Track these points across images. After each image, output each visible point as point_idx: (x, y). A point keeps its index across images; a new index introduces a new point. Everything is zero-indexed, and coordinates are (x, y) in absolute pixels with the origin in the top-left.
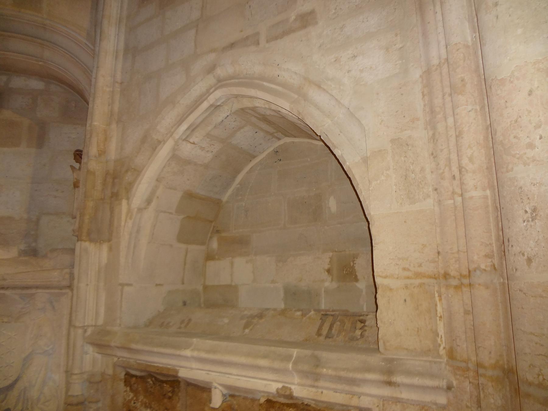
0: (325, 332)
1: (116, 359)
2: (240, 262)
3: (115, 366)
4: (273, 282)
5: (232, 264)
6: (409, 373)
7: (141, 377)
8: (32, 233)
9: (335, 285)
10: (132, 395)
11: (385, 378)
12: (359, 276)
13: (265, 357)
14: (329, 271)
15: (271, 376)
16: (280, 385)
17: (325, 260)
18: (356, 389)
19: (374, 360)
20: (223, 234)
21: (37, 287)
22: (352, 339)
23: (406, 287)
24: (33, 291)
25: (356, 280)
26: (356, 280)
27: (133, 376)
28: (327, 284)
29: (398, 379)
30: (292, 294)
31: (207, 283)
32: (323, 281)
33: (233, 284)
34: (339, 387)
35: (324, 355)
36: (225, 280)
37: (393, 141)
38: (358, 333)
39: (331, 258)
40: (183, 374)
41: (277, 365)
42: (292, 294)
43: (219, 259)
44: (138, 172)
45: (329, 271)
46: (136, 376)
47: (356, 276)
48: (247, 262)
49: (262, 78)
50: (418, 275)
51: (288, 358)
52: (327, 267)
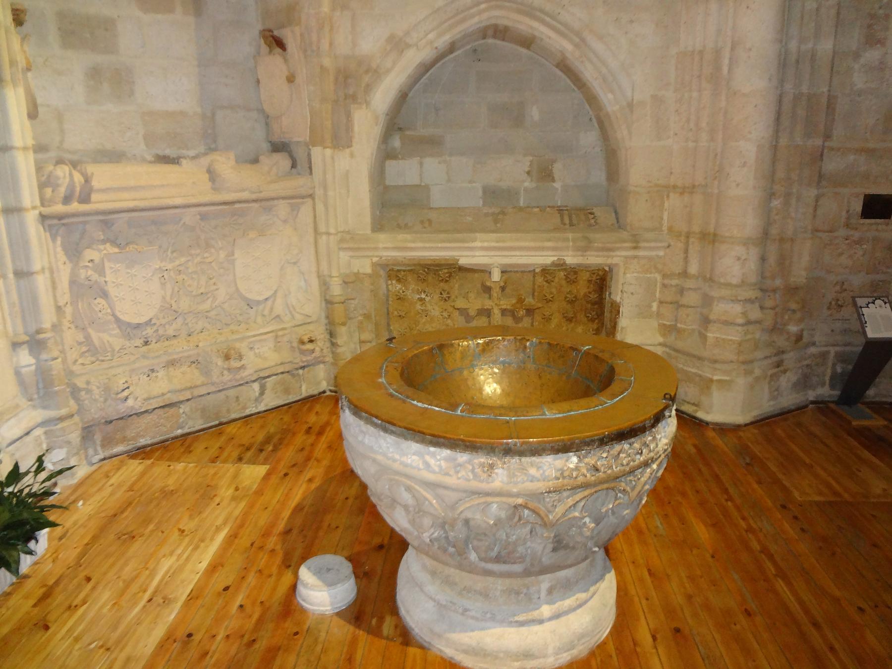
0: (567, 221)
1: (375, 260)
2: (431, 163)
3: (374, 265)
4: (470, 182)
5: (421, 164)
6: (647, 241)
7: (410, 271)
8: (210, 131)
9: (534, 185)
10: (399, 286)
11: (634, 245)
12: (556, 176)
13: (549, 240)
14: (528, 173)
15: (550, 253)
16: (556, 258)
17: (526, 163)
18: (611, 253)
19: (624, 235)
20: (408, 133)
21: (277, 199)
22: (590, 225)
23: (649, 192)
24: (271, 203)
25: (553, 180)
26: (553, 180)
27: (399, 271)
28: (526, 184)
29: (642, 244)
30: (491, 194)
31: (387, 183)
32: (524, 181)
33: (423, 184)
34: (601, 253)
35: (591, 236)
36: (411, 178)
37: (652, 96)
38: (592, 221)
39: (531, 161)
40: (463, 261)
41: (560, 244)
42: (491, 194)
43: (402, 159)
44: (377, 74)
45: (528, 173)
46: (404, 271)
47: (553, 178)
48: (439, 163)
49: (542, 11)
50: (656, 185)
51: (567, 240)
52: (527, 169)
